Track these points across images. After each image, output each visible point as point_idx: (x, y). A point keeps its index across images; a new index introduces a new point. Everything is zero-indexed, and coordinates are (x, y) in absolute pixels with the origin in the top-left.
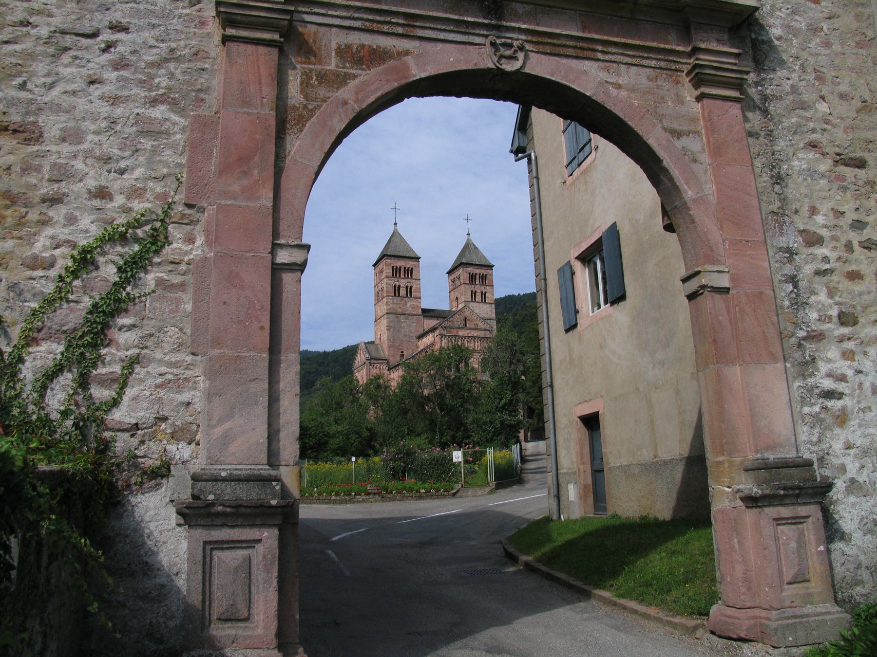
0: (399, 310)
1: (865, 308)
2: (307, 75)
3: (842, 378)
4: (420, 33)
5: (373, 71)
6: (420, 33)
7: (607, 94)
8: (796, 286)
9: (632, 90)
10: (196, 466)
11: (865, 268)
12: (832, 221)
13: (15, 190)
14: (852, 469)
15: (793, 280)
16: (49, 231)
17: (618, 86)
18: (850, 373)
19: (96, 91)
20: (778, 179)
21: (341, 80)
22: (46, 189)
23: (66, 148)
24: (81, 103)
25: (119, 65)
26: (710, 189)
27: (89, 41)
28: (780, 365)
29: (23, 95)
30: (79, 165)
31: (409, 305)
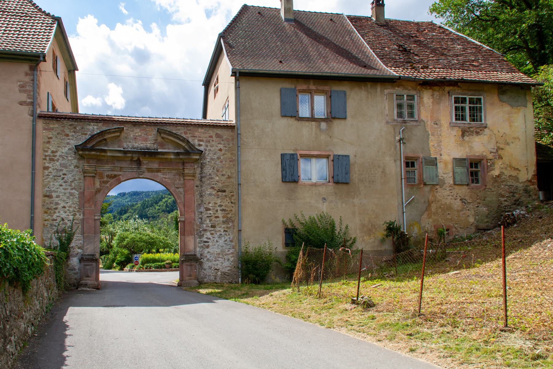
1: (218, 224)
2: (100, 182)
3: (210, 239)
4: (123, 170)
5: (114, 180)
6: (123, 170)
7: (162, 180)
8: (201, 220)
9: (169, 178)
10: (82, 253)
11: (220, 215)
12: (213, 205)
13: (49, 207)
14: (208, 257)
15: (201, 219)
16: (56, 214)
17: (166, 178)
18: (211, 238)
19: (61, 188)
20: (201, 196)
21: (106, 182)
22: (54, 207)
23: (57, 199)
24: (59, 190)
25: (65, 182)
27: (59, 178)
28: (193, 236)
29: (49, 189)
30: (60, 202)
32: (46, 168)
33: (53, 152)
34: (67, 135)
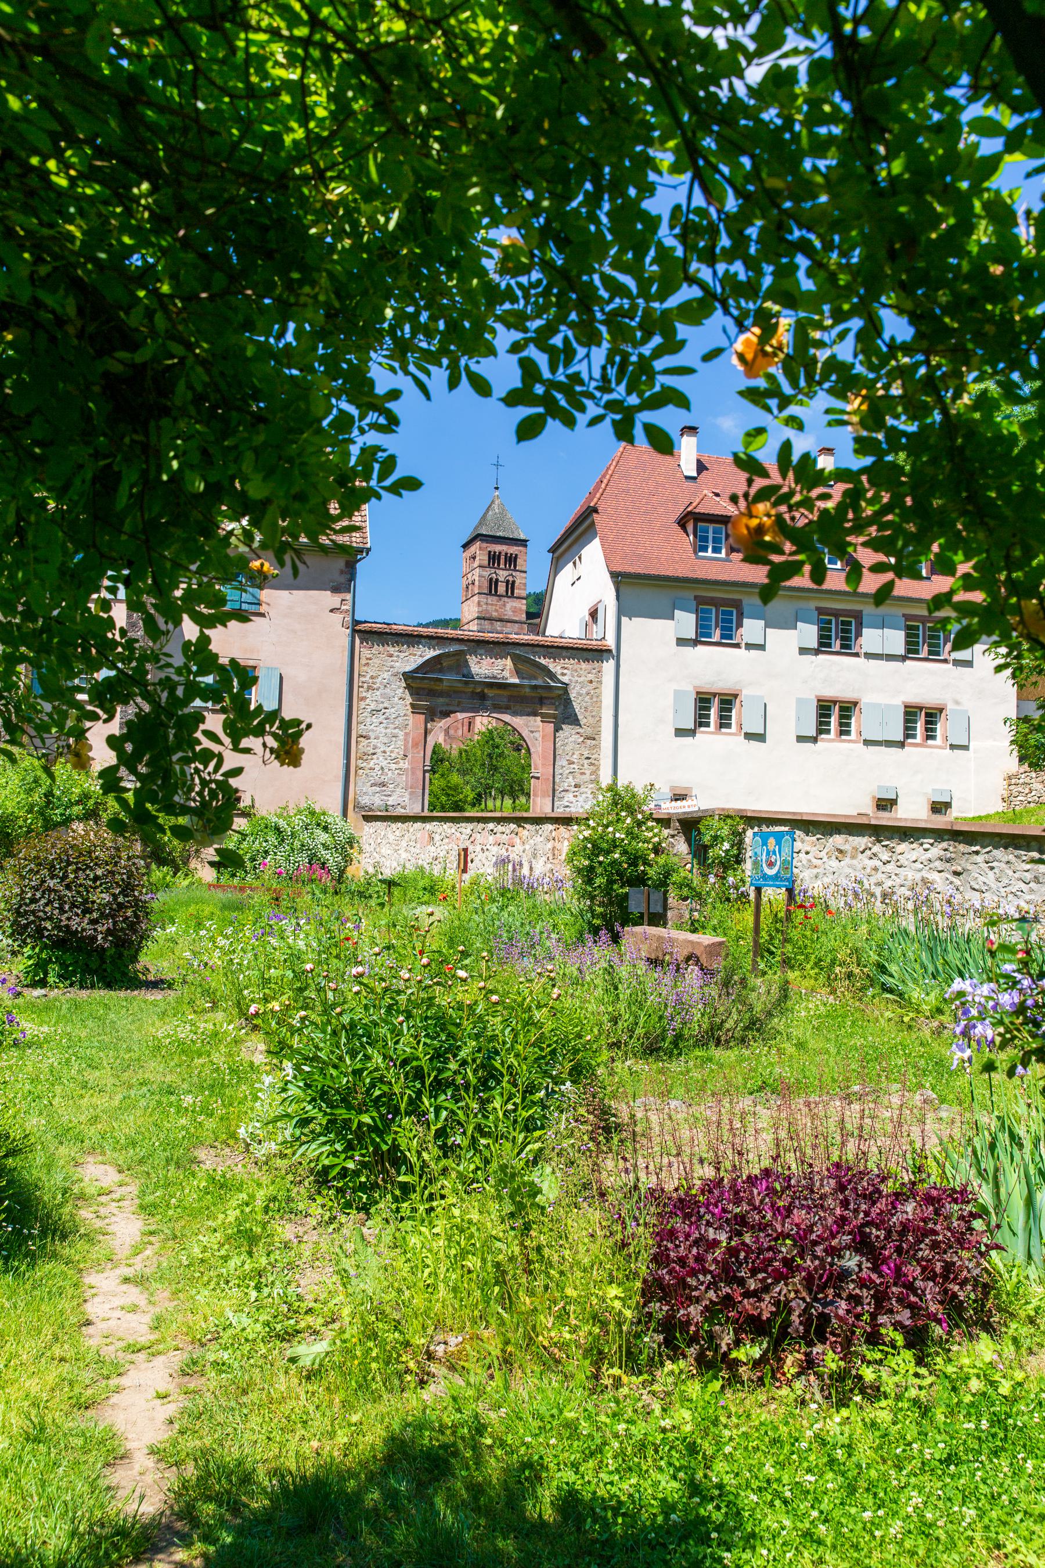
0: (495, 614)
26: (540, 749)
31: (508, 606)
32: (364, 699)
33: (372, 677)
34: (391, 656)
